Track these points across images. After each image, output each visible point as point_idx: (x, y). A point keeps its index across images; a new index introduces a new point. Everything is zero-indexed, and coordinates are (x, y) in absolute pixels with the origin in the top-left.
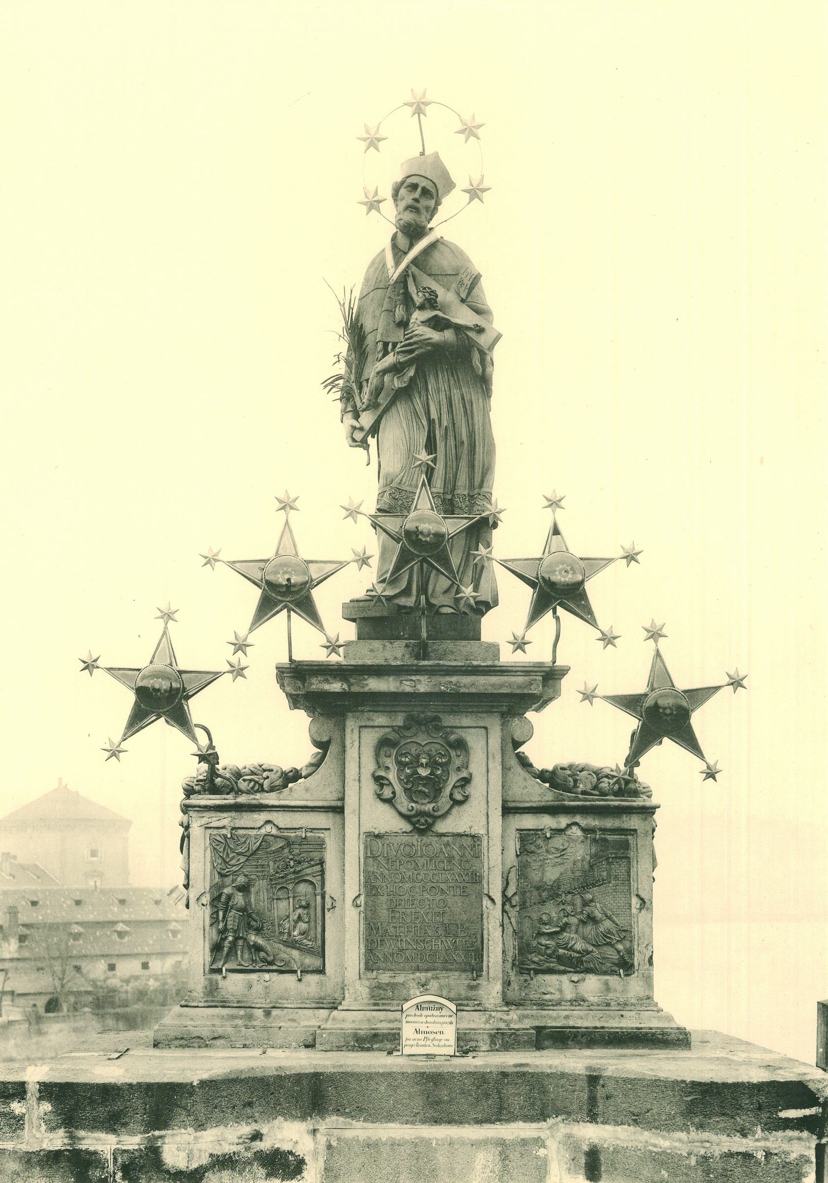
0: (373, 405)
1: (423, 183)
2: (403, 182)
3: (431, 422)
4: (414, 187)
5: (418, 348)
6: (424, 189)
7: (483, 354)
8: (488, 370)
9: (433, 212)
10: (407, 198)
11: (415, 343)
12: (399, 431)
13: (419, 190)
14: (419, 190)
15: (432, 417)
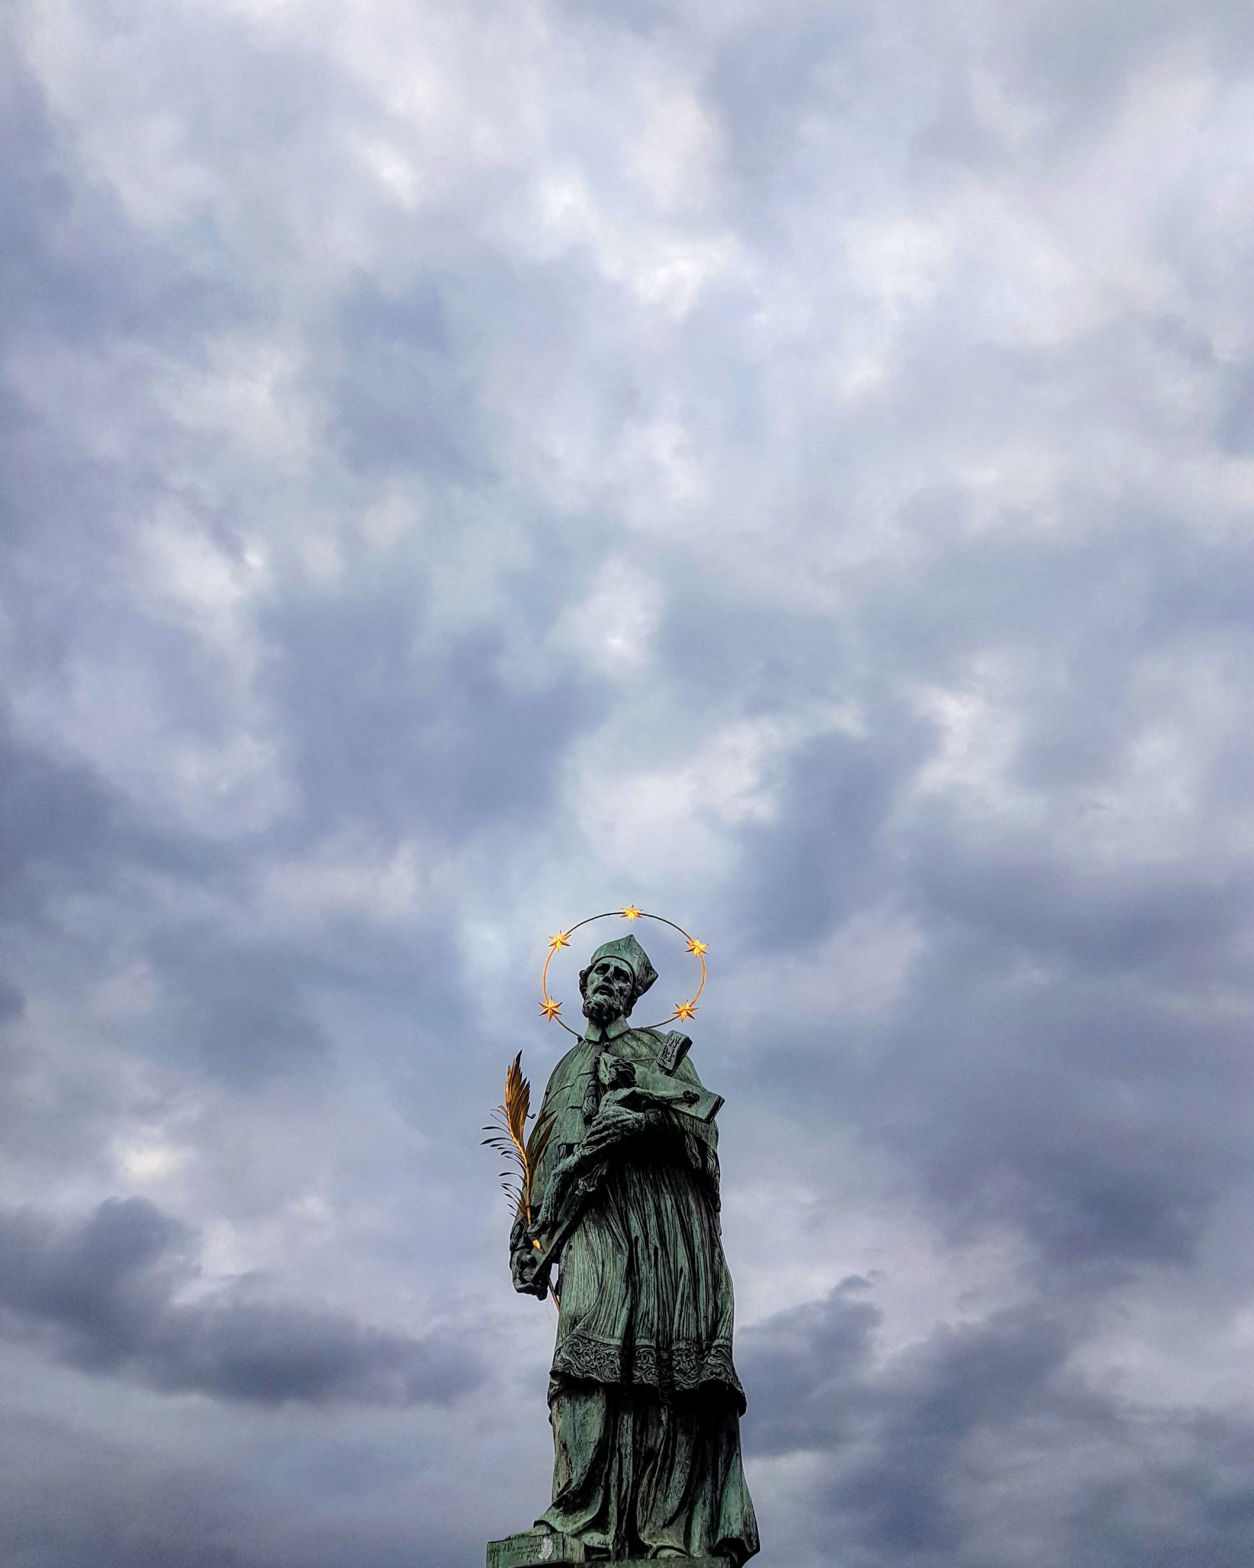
0: (549, 1227)
1: (614, 963)
2: (591, 969)
3: (632, 1244)
4: (605, 968)
5: (609, 1135)
6: (616, 968)
7: (703, 1148)
8: (711, 1163)
9: (631, 1001)
10: (596, 979)
11: (606, 1128)
12: (588, 1260)
13: (612, 969)
14: (612, 969)
15: (633, 1236)
